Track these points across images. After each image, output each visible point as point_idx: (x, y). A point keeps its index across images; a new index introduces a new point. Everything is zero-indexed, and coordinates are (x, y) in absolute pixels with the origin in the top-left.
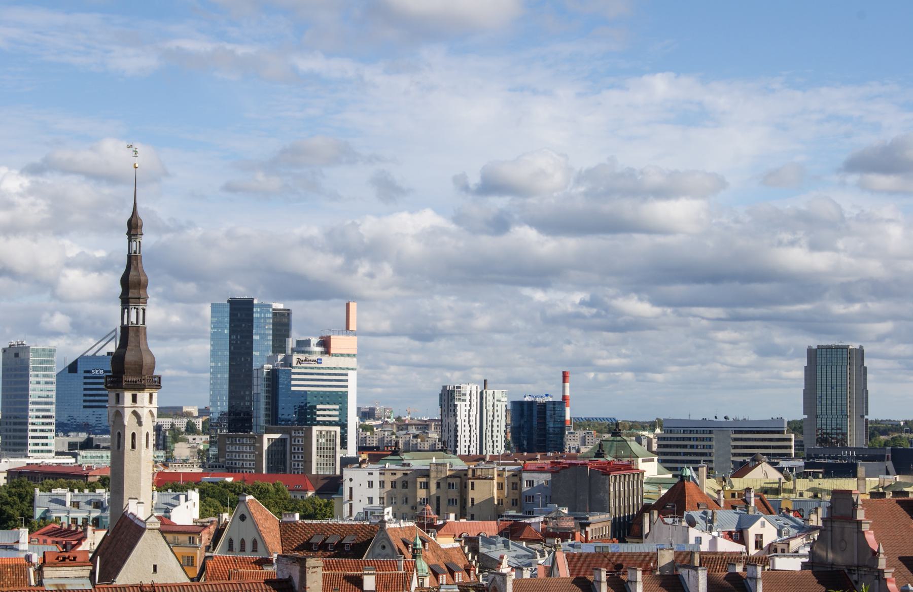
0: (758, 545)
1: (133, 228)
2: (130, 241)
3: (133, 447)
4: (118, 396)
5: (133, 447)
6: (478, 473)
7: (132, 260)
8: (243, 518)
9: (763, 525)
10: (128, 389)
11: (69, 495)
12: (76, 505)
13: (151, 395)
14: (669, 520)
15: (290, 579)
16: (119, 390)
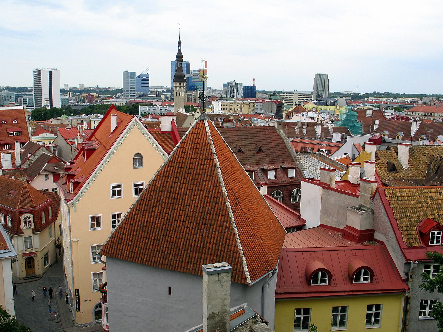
0: (318, 121)
1: (180, 43)
2: (178, 47)
3: (180, 96)
4: (176, 84)
5: (180, 96)
6: (245, 103)
7: (180, 51)
8: (198, 113)
9: (319, 116)
10: (178, 82)
11: (147, 107)
12: (149, 110)
13: (184, 84)
14: (297, 115)
15: (274, 126)
16: (176, 83)
